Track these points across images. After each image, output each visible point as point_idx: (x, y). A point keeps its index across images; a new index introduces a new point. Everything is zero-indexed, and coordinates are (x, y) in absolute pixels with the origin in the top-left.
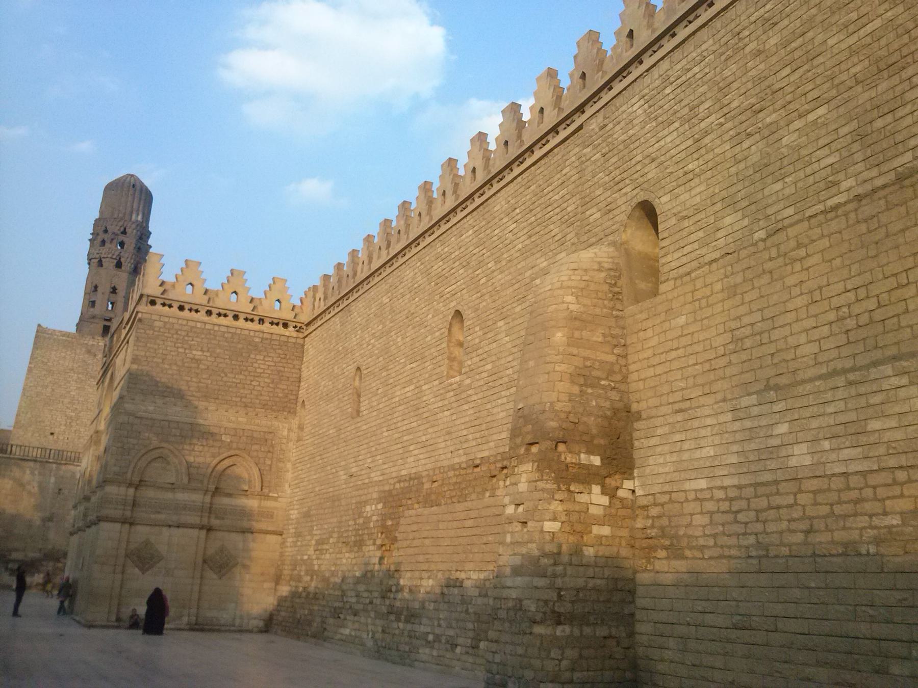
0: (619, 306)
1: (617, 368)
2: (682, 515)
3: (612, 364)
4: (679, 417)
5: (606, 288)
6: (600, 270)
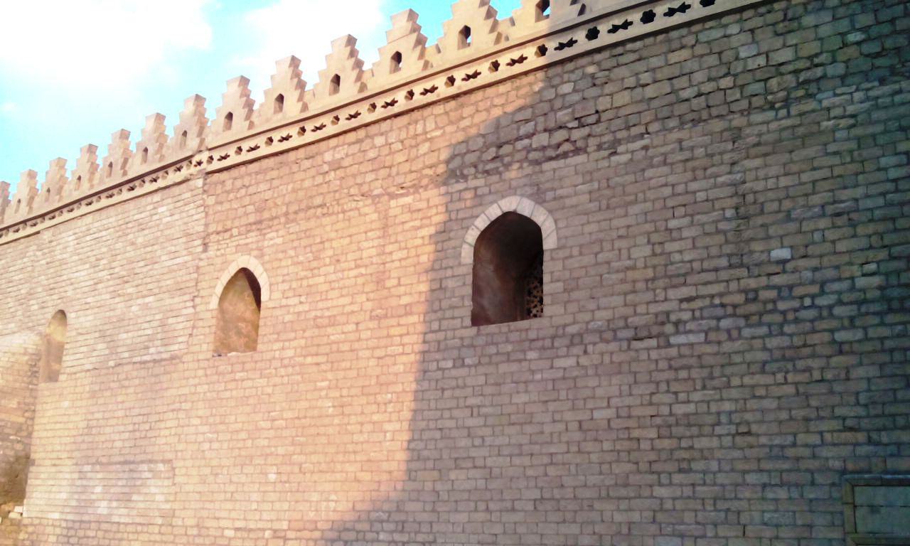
0: (35, 382)
1: (24, 427)
2: (44, 534)
3: (21, 424)
4: (54, 469)
5: (27, 368)
6: (25, 354)
